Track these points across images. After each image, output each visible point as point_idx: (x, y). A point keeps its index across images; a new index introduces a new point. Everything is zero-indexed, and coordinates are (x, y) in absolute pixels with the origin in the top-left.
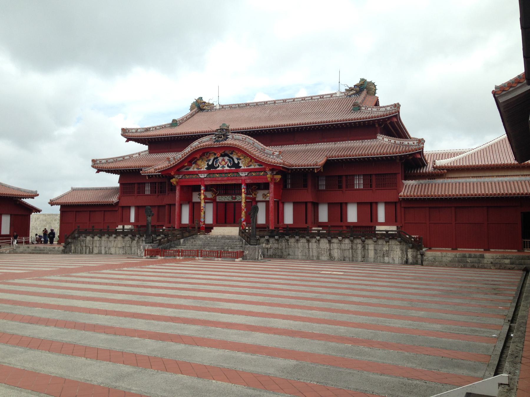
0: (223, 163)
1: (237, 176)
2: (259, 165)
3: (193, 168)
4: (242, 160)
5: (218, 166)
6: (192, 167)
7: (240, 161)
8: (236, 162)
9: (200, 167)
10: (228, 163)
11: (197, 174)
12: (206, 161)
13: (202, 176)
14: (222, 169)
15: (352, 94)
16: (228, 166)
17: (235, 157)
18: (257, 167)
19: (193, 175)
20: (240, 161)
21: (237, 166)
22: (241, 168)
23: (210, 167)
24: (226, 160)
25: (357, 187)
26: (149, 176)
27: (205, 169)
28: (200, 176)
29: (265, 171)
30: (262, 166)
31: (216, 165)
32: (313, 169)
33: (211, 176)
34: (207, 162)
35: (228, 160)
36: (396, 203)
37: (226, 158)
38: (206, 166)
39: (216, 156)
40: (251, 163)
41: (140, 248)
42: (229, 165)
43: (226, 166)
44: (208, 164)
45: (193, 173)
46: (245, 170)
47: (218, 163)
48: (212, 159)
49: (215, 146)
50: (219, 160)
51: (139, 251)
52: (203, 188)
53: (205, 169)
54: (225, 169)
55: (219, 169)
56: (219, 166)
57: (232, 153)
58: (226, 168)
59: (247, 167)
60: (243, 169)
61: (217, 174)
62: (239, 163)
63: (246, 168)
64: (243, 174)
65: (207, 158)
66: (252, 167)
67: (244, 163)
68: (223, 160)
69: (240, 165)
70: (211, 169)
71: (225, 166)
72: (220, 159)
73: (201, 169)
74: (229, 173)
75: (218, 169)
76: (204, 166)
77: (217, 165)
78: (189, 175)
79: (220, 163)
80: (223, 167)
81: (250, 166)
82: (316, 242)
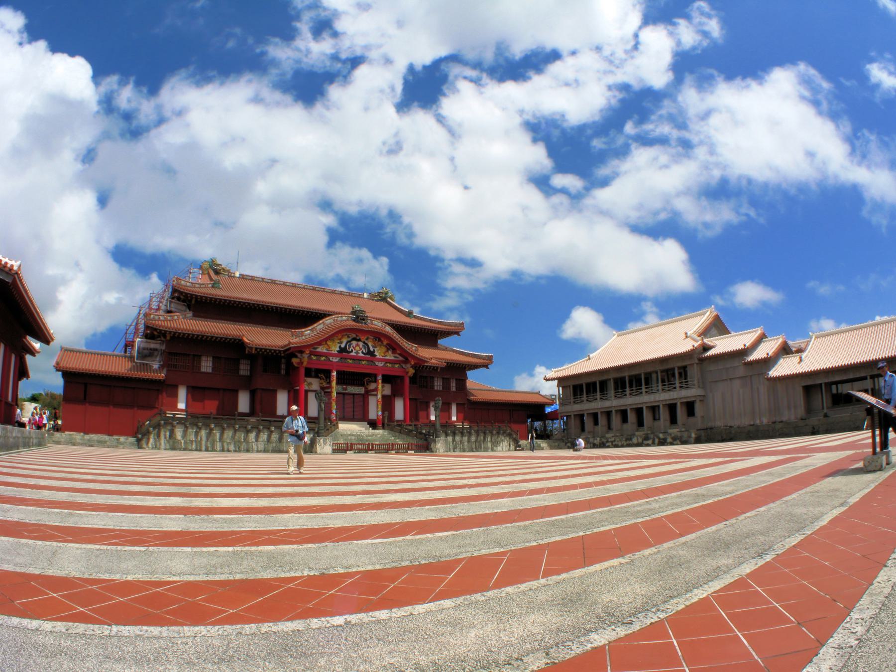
0: (358, 348)
1: (371, 365)
2: (395, 357)
3: (321, 349)
4: (378, 348)
5: (352, 351)
6: (321, 347)
7: (376, 349)
8: (372, 349)
9: (330, 349)
10: (363, 349)
11: (326, 357)
12: (338, 343)
13: (335, 360)
14: (355, 354)
15: (378, 299)
16: (362, 352)
17: (370, 344)
18: (393, 358)
19: (321, 356)
20: (376, 349)
21: (372, 354)
22: (377, 357)
23: (342, 350)
24: (361, 346)
25: (436, 388)
26: (256, 349)
27: (336, 352)
28: (331, 360)
29: (400, 364)
30: (398, 358)
31: (349, 349)
32: (437, 368)
33: (343, 360)
34: (339, 345)
35: (363, 346)
36: (464, 404)
37: (361, 344)
38: (338, 349)
39: (349, 339)
40: (387, 354)
41: (319, 441)
42: (364, 351)
43: (360, 352)
44: (340, 347)
45: (319, 355)
46: (380, 360)
47: (352, 348)
48: (345, 341)
49: (364, 329)
50: (352, 344)
51: (318, 446)
52: (335, 374)
53: (336, 352)
54: (359, 355)
55: (352, 354)
56: (352, 350)
57: (367, 339)
58: (361, 354)
59: (383, 356)
60: (378, 358)
61: (350, 359)
62: (374, 350)
63: (381, 357)
64: (380, 364)
65: (340, 339)
66: (388, 358)
67: (379, 351)
68: (358, 345)
69: (376, 353)
70: (344, 354)
71: (359, 352)
72: (354, 343)
73: (331, 351)
74: (363, 361)
75: (352, 354)
76: (335, 349)
77: (350, 350)
78: (316, 356)
79: (354, 348)
80: (357, 353)
81: (386, 356)
82: (452, 436)
